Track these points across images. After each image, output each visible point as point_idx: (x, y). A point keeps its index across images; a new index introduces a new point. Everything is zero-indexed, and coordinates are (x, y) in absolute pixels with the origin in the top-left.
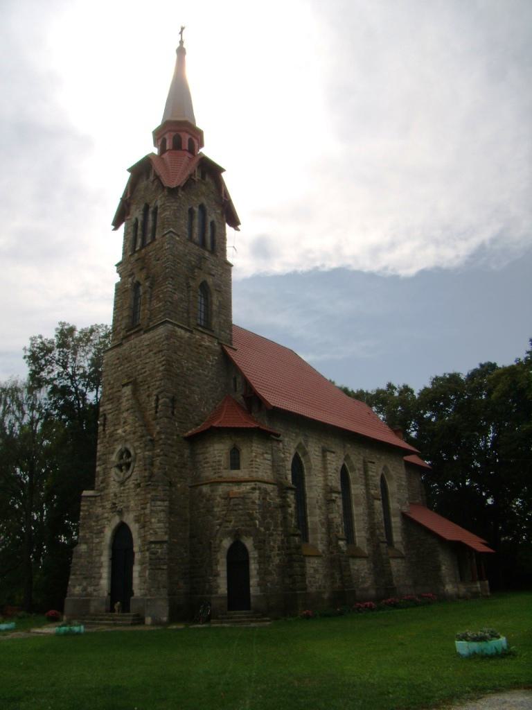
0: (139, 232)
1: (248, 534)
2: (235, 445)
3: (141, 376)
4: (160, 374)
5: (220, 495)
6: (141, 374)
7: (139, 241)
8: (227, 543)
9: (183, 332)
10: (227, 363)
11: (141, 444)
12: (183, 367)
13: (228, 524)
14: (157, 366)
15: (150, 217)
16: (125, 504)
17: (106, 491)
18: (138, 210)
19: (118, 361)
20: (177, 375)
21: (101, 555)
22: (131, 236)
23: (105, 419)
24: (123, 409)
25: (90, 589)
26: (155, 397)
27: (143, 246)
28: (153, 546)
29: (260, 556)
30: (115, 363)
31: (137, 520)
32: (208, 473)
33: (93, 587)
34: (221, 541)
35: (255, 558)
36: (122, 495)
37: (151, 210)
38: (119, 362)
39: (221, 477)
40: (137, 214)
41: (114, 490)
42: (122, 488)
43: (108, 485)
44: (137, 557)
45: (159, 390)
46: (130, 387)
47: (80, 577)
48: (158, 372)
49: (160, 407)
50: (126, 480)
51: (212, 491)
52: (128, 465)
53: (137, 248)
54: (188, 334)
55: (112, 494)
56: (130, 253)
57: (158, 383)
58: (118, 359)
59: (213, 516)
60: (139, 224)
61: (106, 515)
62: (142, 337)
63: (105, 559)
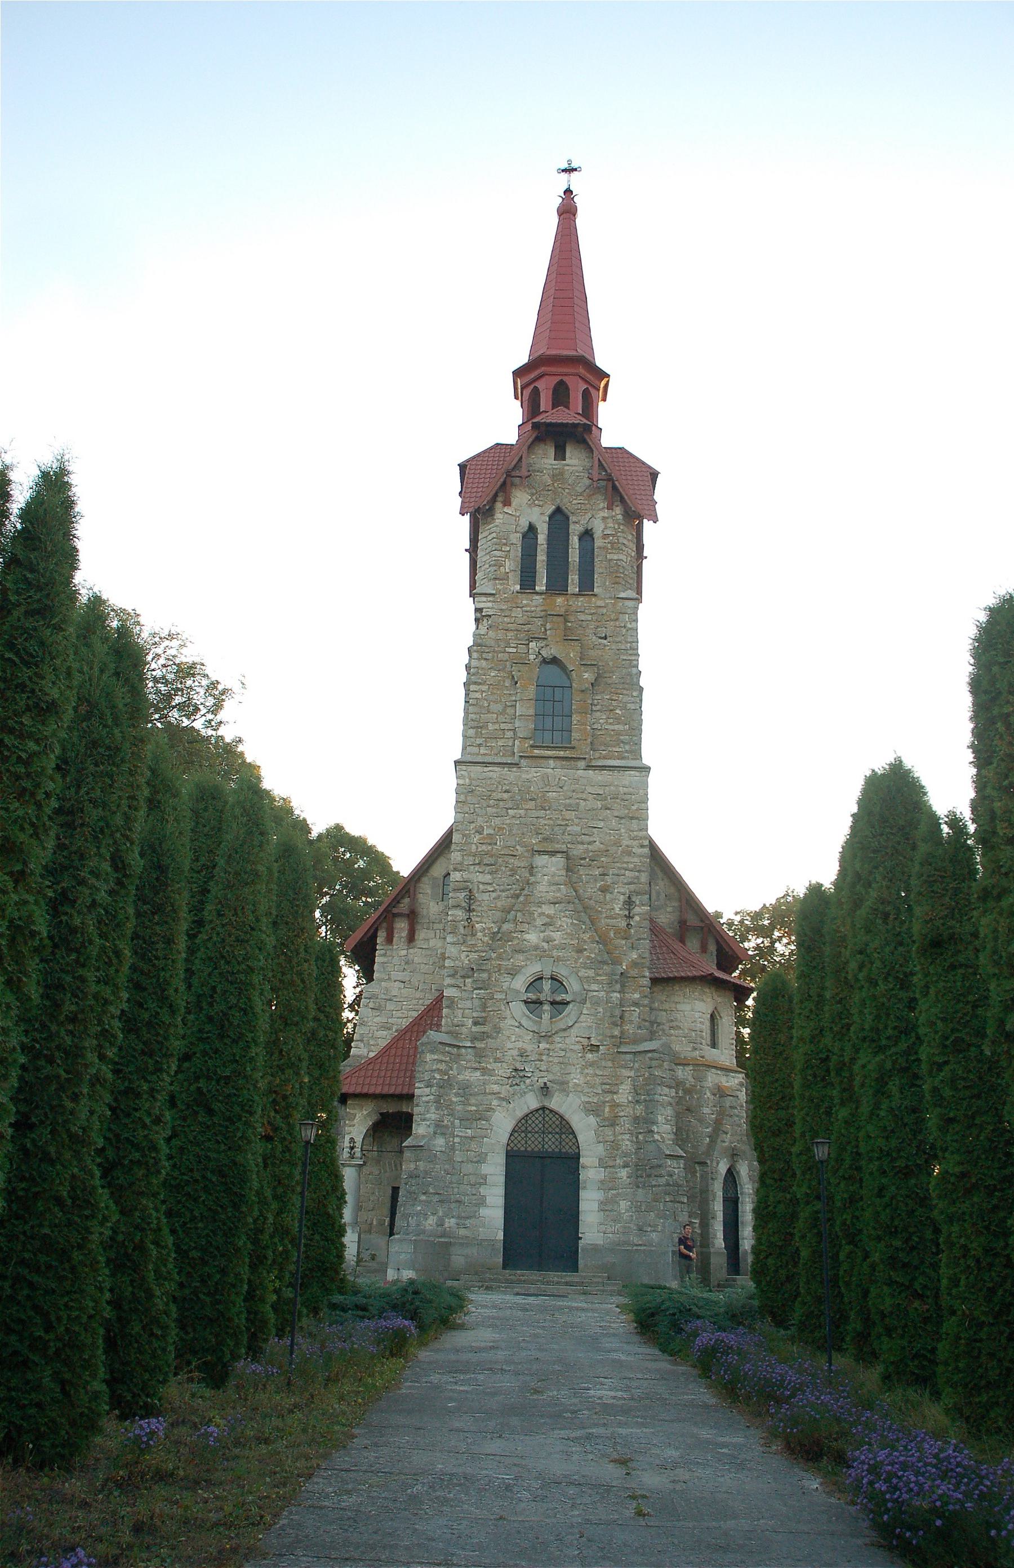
0: (541, 557)
2: (716, 1008)
3: (581, 847)
4: (636, 860)
6: (583, 843)
14: (625, 843)
15: (574, 541)
16: (551, 1077)
18: (536, 509)
19: (506, 796)
21: (481, 1159)
23: (471, 898)
25: (450, 1223)
28: (669, 1162)
30: (496, 795)
31: (592, 1110)
33: (453, 1220)
37: (575, 530)
38: (512, 799)
39: (703, 1057)
41: (520, 1045)
42: (543, 1046)
43: (498, 1030)
44: (591, 1172)
45: (632, 887)
46: (559, 861)
47: (436, 1198)
49: (637, 918)
50: (556, 1033)
52: (558, 1005)
55: (515, 1052)
59: (701, 1120)
60: (542, 538)
61: (496, 1088)
63: (495, 1169)
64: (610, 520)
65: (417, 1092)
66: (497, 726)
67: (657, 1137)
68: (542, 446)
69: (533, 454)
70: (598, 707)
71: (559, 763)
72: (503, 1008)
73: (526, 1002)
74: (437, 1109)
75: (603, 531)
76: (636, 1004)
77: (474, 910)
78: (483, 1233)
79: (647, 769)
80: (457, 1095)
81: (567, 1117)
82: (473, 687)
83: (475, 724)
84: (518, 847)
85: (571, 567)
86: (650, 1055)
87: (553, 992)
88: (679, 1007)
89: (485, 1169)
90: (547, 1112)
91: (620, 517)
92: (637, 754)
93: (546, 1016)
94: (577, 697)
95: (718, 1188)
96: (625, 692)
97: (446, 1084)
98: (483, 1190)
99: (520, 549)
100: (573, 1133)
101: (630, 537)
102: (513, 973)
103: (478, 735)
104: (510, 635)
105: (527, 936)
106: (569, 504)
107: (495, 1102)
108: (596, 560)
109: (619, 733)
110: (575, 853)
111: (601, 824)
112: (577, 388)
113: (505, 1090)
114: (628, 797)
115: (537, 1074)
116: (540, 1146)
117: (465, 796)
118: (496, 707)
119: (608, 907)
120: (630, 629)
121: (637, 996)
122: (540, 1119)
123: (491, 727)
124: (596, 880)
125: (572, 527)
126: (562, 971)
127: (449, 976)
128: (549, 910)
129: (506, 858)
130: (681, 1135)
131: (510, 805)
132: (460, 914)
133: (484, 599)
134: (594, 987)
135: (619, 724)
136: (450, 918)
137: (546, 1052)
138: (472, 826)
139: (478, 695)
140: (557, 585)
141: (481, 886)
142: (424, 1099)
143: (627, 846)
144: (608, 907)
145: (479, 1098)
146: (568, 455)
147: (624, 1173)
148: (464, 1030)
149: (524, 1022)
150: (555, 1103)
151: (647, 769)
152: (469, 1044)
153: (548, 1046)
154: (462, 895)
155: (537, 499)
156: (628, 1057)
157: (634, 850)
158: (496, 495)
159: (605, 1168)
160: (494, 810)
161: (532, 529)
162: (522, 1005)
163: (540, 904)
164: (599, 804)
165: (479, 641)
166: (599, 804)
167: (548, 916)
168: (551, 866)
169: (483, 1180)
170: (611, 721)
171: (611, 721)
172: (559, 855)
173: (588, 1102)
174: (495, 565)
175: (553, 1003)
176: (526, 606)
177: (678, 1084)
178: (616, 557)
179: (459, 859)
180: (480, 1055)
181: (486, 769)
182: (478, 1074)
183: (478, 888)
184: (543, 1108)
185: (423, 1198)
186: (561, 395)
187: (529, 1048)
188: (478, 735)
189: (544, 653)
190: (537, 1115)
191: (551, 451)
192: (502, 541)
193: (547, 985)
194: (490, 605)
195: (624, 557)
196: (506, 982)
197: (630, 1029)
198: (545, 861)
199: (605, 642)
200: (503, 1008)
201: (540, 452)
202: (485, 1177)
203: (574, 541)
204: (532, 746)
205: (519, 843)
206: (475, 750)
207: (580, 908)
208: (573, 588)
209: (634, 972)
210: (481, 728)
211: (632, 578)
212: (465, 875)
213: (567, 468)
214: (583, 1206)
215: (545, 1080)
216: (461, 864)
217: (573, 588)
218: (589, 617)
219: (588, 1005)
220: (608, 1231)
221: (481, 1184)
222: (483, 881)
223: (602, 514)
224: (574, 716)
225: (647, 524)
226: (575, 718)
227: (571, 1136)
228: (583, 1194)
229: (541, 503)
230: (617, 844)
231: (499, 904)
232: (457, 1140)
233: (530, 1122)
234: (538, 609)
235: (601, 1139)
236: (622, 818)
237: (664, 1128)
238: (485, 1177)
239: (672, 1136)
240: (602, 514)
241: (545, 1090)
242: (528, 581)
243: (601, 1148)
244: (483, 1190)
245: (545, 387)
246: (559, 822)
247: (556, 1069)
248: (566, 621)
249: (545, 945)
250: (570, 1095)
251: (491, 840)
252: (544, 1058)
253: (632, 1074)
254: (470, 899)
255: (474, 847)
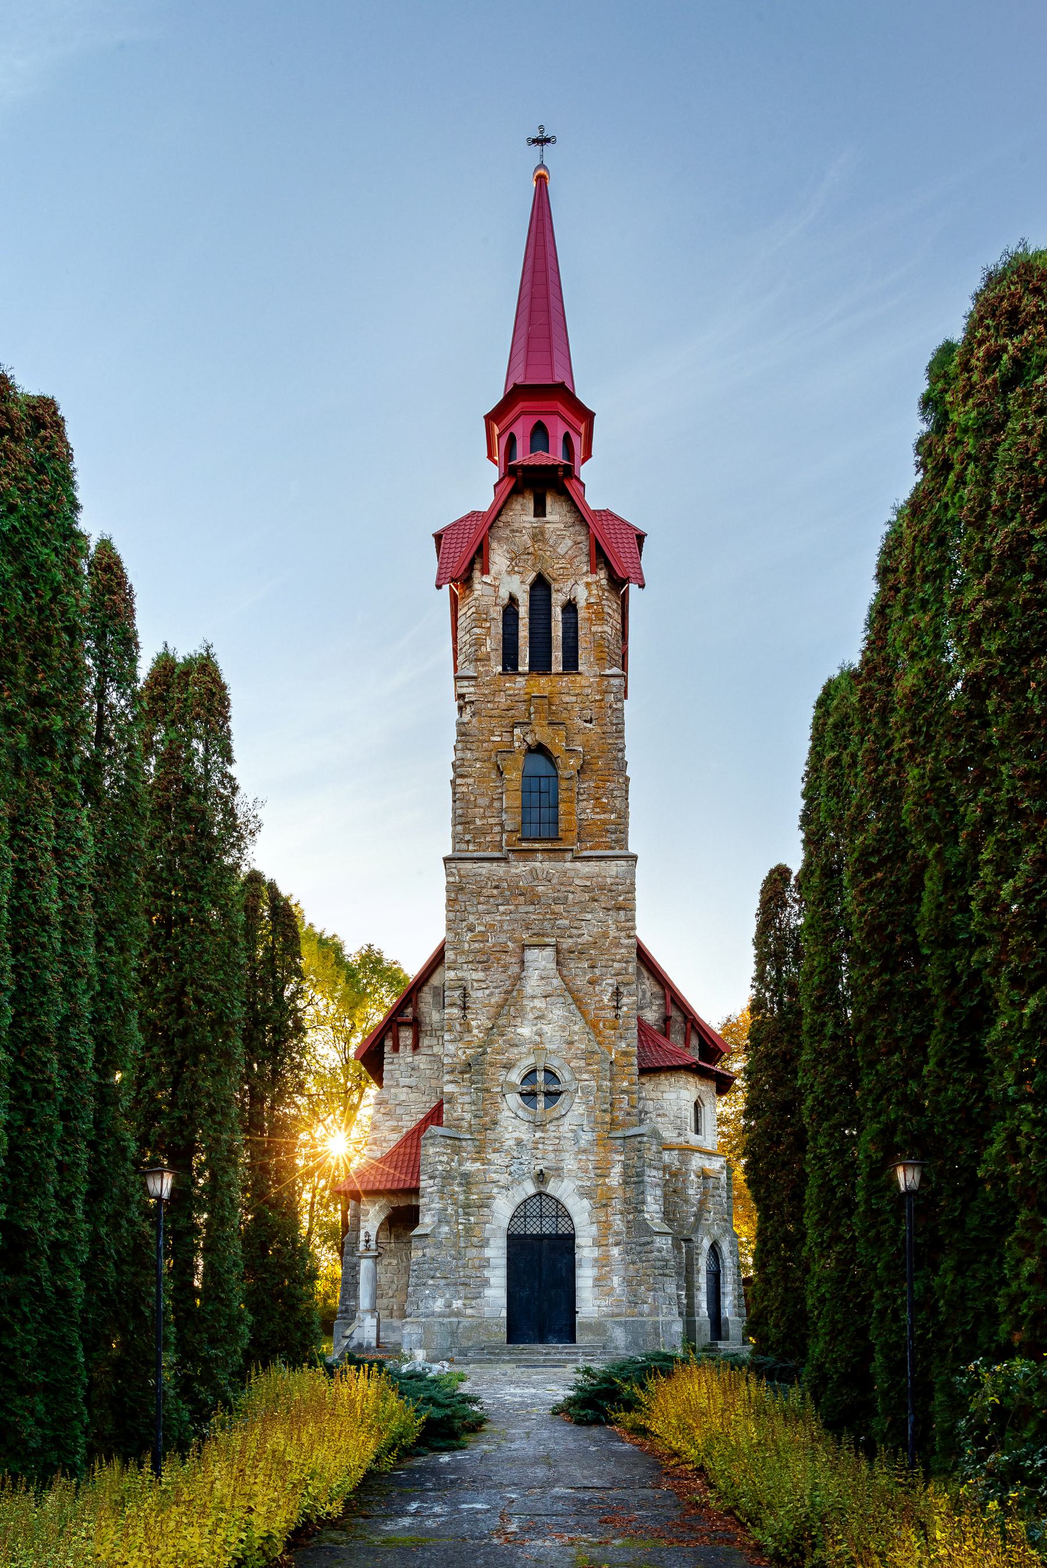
0: (524, 633)
3: (570, 940)
4: (623, 951)
6: (570, 937)
11: (589, 1064)
15: (557, 613)
16: (546, 1164)
17: (491, 1135)
18: (517, 578)
19: (495, 892)
21: (484, 1244)
24: (529, 990)
25: (457, 1304)
26: (610, 989)
30: (486, 892)
31: (585, 1193)
33: (460, 1302)
36: (540, 1146)
37: (558, 599)
41: (516, 1135)
43: (495, 1123)
44: (586, 1251)
47: (442, 1282)
48: (618, 945)
49: (625, 1009)
50: (551, 1122)
52: (553, 1096)
55: (512, 1142)
57: (616, 965)
58: (496, 887)
60: (523, 611)
62: (568, 865)
63: (497, 1252)
64: (594, 587)
65: (422, 1184)
66: (485, 821)
67: (647, 1216)
68: (520, 499)
69: (512, 510)
70: (585, 796)
71: (546, 855)
72: (499, 1100)
73: (521, 1094)
74: (441, 1198)
75: (587, 600)
76: (623, 1092)
77: (469, 1008)
78: (487, 1311)
79: (634, 858)
80: (460, 1184)
81: (562, 1200)
82: (459, 781)
83: (463, 819)
84: (509, 943)
85: (554, 643)
86: (639, 1139)
87: (547, 1082)
89: (488, 1252)
90: (544, 1197)
91: (604, 582)
92: (623, 843)
93: (541, 1105)
94: (564, 784)
95: (703, 1263)
96: (611, 778)
97: (448, 1177)
98: (486, 1273)
99: (501, 625)
100: (569, 1216)
101: (615, 606)
102: (508, 1067)
103: (466, 831)
104: (494, 722)
105: (519, 1030)
106: (553, 570)
107: (495, 1190)
108: (580, 633)
109: (604, 822)
110: (565, 946)
111: (589, 916)
112: (558, 430)
113: (504, 1179)
114: (614, 887)
115: (534, 1162)
116: (538, 1229)
117: (456, 893)
118: (483, 801)
119: (597, 998)
120: (617, 709)
121: (625, 1084)
122: (538, 1204)
123: (478, 822)
124: (585, 973)
125: (554, 596)
126: (554, 1063)
127: (448, 1073)
128: (539, 1003)
129: (498, 955)
130: (668, 1216)
131: (500, 901)
132: (455, 1011)
133: (466, 683)
134: (585, 1076)
135: (605, 812)
136: (446, 1017)
137: (541, 1141)
138: (465, 923)
139: (464, 789)
140: (541, 664)
141: (475, 984)
142: (429, 1190)
143: (615, 938)
144: (597, 998)
145: (481, 1186)
146: (548, 509)
147: (615, 1251)
148: (465, 1124)
149: (520, 1113)
150: (551, 1189)
151: (634, 858)
152: (469, 1137)
153: (542, 1135)
154: (458, 993)
155: (517, 565)
156: (619, 1142)
157: (622, 941)
158: (472, 562)
159: (599, 1246)
160: (485, 907)
161: (513, 600)
162: (518, 1097)
163: (533, 997)
164: (587, 896)
165: (463, 729)
166: (587, 896)
167: (540, 1009)
168: (541, 960)
169: (485, 1264)
170: (598, 810)
171: (598, 810)
172: (549, 949)
173: (582, 1187)
174: (475, 645)
175: (548, 1094)
176: (509, 689)
177: (665, 1168)
178: (600, 629)
179: (453, 957)
180: (480, 1150)
181: (475, 865)
182: (478, 1164)
183: (472, 986)
184: (540, 1194)
185: (431, 1282)
186: (540, 434)
187: (525, 1137)
188: (466, 831)
189: (529, 739)
190: (535, 1200)
191: (531, 506)
192: (481, 618)
193: (541, 1077)
194: (472, 689)
195: (609, 629)
196: (502, 1075)
197: (620, 1115)
198: (535, 956)
199: (588, 725)
200: (499, 1100)
201: (518, 507)
202: (488, 1260)
203: (557, 613)
204: (519, 839)
205: (510, 939)
206: (464, 846)
207: (570, 1001)
208: (557, 667)
209: (623, 1061)
210: (468, 823)
211: (617, 654)
212: (460, 974)
213: (548, 526)
214: (580, 1283)
215: (541, 1167)
216: (455, 962)
217: (557, 667)
218: (574, 699)
219: (580, 1094)
220: (603, 1303)
221: (484, 1267)
222: (476, 978)
223: (585, 579)
224: (560, 806)
225: (633, 588)
226: (562, 808)
227: (566, 1219)
228: (579, 1272)
229: (521, 569)
230: (605, 935)
231: (493, 1000)
232: (461, 1227)
233: (528, 1207)
234: (522, 692)
235: (594, 1220)
236: (609, 910)
237: (653, 1208)
238: (488, 1260)
239: (661, 1215)
240: (585, 579)
241: (541, 1177)
242: (510, 661)
243: (594, 1228)
244: (486, 1273)
245: (522, 430)
246: (548, 916)
247: (551, 1156)
248: (550, 704)
249: (537, 1037)
250: (566, 1180)
251: (483, 937)
252: (540, 1146)
253: (622, 1158)
254: (465, 997)
255: (466, 945)
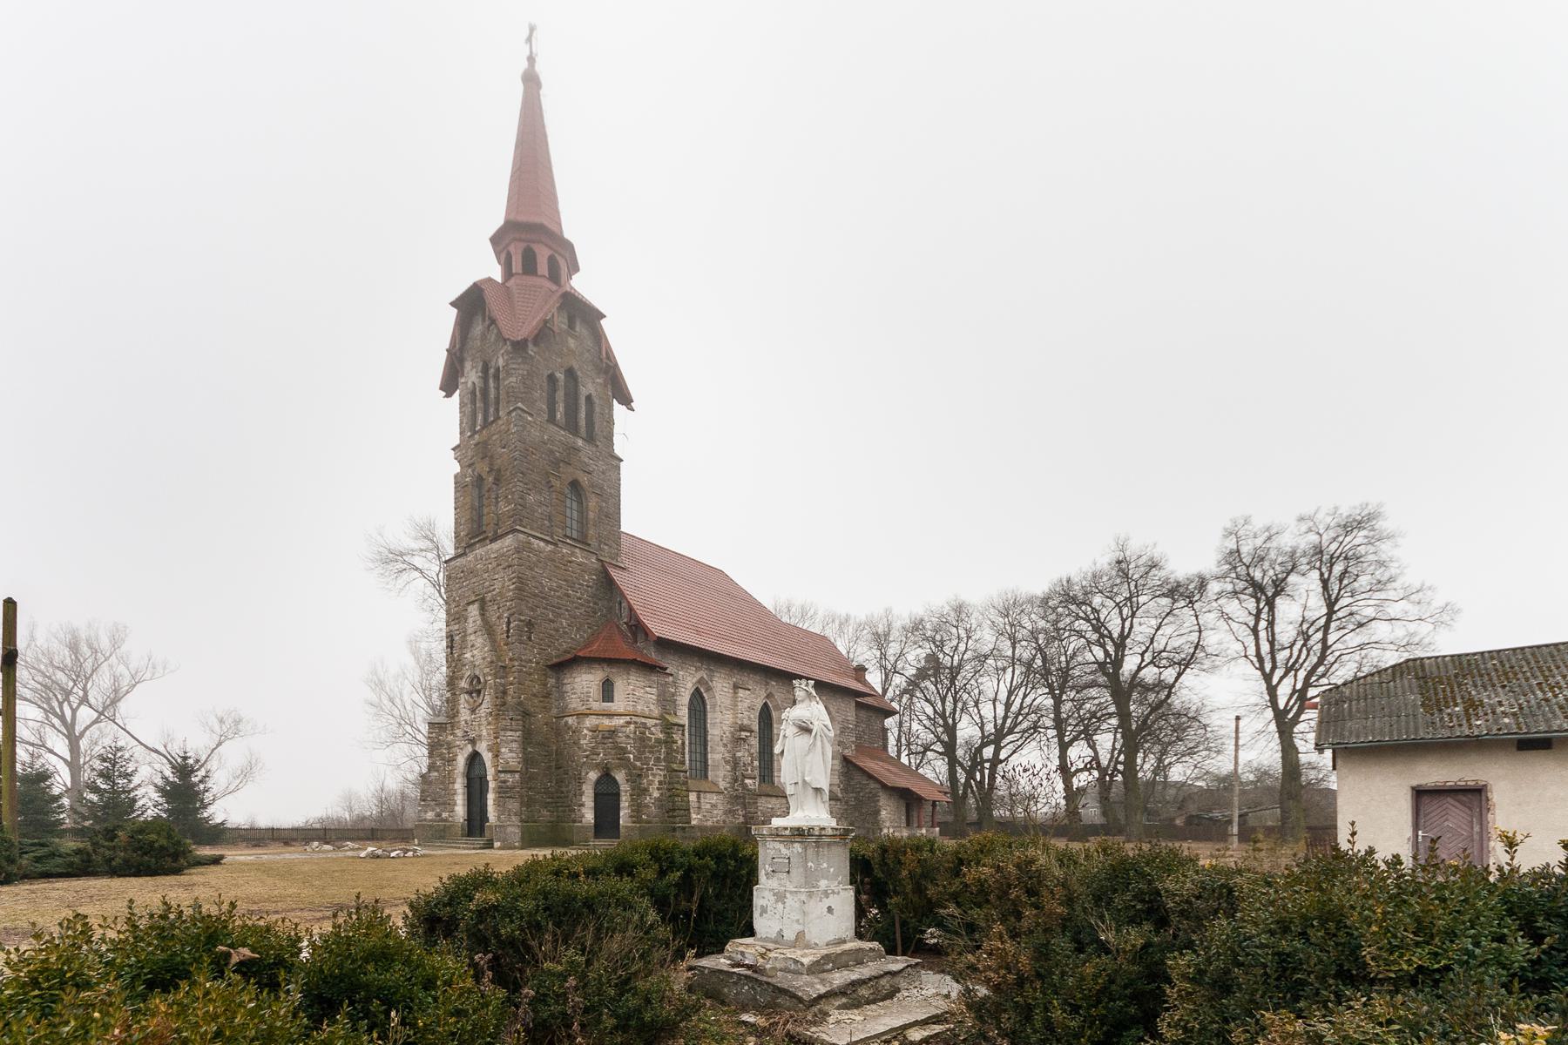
1: (619, 767)
5: (587, 729)
7: (480, 417)
8: (593, 776)
9: (542, 544)
10: (607, 585)
12: (543, 587)
13: (595, 757)
20: (535, 595)
22: (468, 409)
27: (486, 425)
29: (633, 789)
32: (574, 704)
34: (587, 773)
35: (626, 791)
40: (472, 376)
51: (578, 723)
53: (478, 428)
54: (550, 548)
56: (469, 434)
60: (478, 393)
62: (489, 547)
88: (576, 680)
111: (497, 576)
